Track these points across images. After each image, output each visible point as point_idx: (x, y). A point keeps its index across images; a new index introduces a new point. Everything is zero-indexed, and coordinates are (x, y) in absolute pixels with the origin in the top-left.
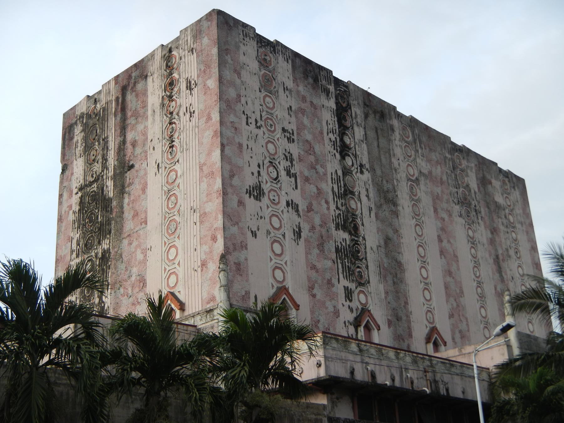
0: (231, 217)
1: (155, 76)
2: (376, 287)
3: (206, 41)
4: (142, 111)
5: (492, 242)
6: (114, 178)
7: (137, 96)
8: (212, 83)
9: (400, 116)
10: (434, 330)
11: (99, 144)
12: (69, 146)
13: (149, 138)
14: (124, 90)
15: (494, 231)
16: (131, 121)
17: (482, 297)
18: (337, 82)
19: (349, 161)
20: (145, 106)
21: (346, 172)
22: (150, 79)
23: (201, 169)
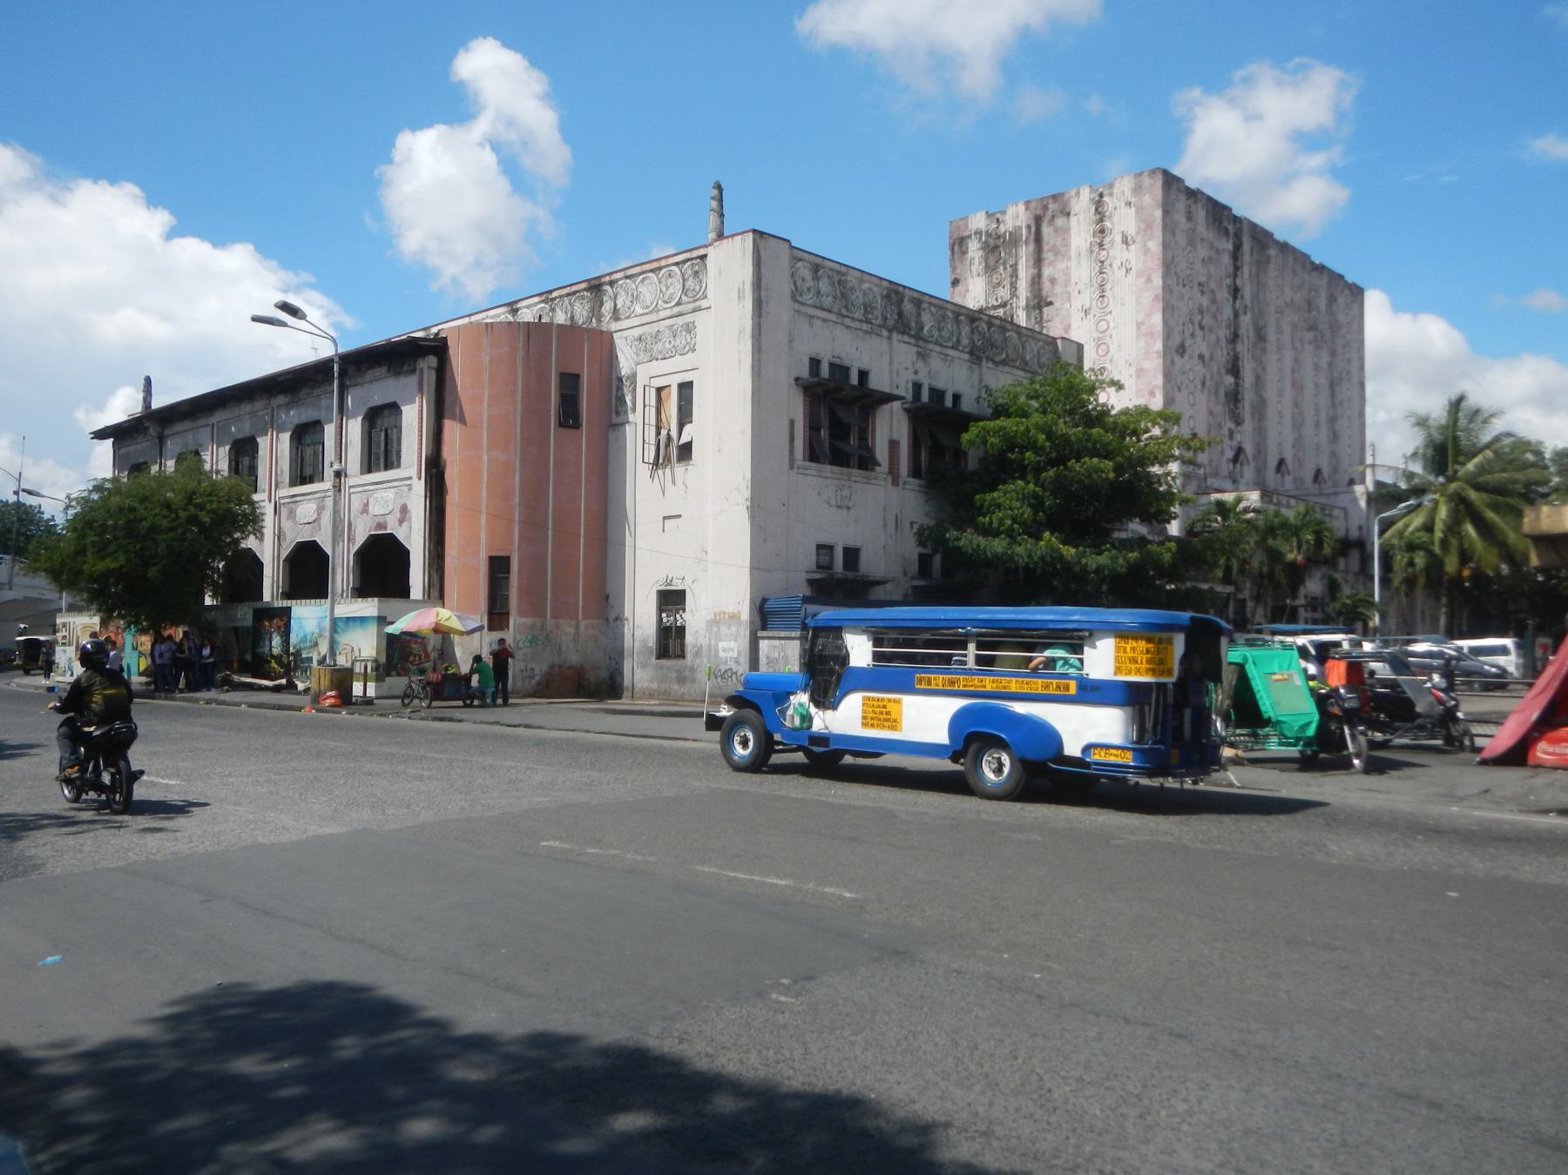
0: (1168, 376)
1: (1082, 217)
2: (1249, 424)
3: (1147, 199)
4: (1063, 250)
5: (1330, 365)
6: (1027, 308)
7: (1056, 230)
8: (1155, 245)
9: (1276, 242)
10: (1281, 462)
12: (962, 261)
13: (1074, 280)
14: (1038, 220)
15: (1333, 353)
16: (1048, 256)
17: (1317, 425)
18: (1235, 217)
19: (1238, 303)
20: (1067, 244)
21: (1236, 315)
22: (1073, 219)
23: (1138, 327)
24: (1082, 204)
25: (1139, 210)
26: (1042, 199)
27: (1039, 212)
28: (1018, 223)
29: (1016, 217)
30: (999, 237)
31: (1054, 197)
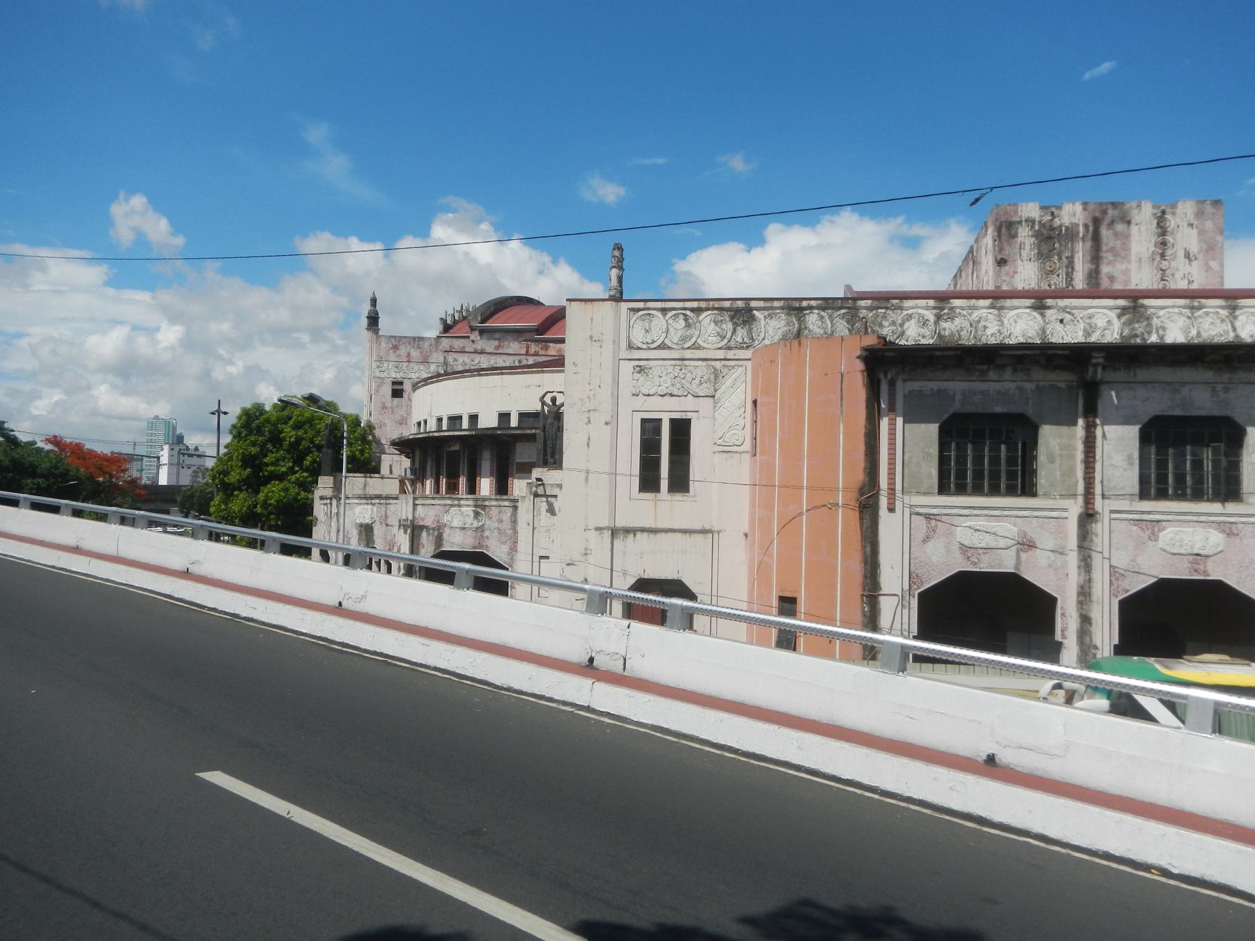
1: (1143, 228)
4: (1123, 253)
7: (1116, 235)
11: (1060, 259)
12: (1010, 244)
14: (1097, 222)
16: (1107, 256)
20: (1126, 247)
22: (1134, 229)
24: (1144, 215)
25: (1201, 232)
26: (1100, 204)
27: (1097, 214)
28: (1075, 220)
29: (1072, 214)
30: (1052, 229)
31: (1115, 205)
